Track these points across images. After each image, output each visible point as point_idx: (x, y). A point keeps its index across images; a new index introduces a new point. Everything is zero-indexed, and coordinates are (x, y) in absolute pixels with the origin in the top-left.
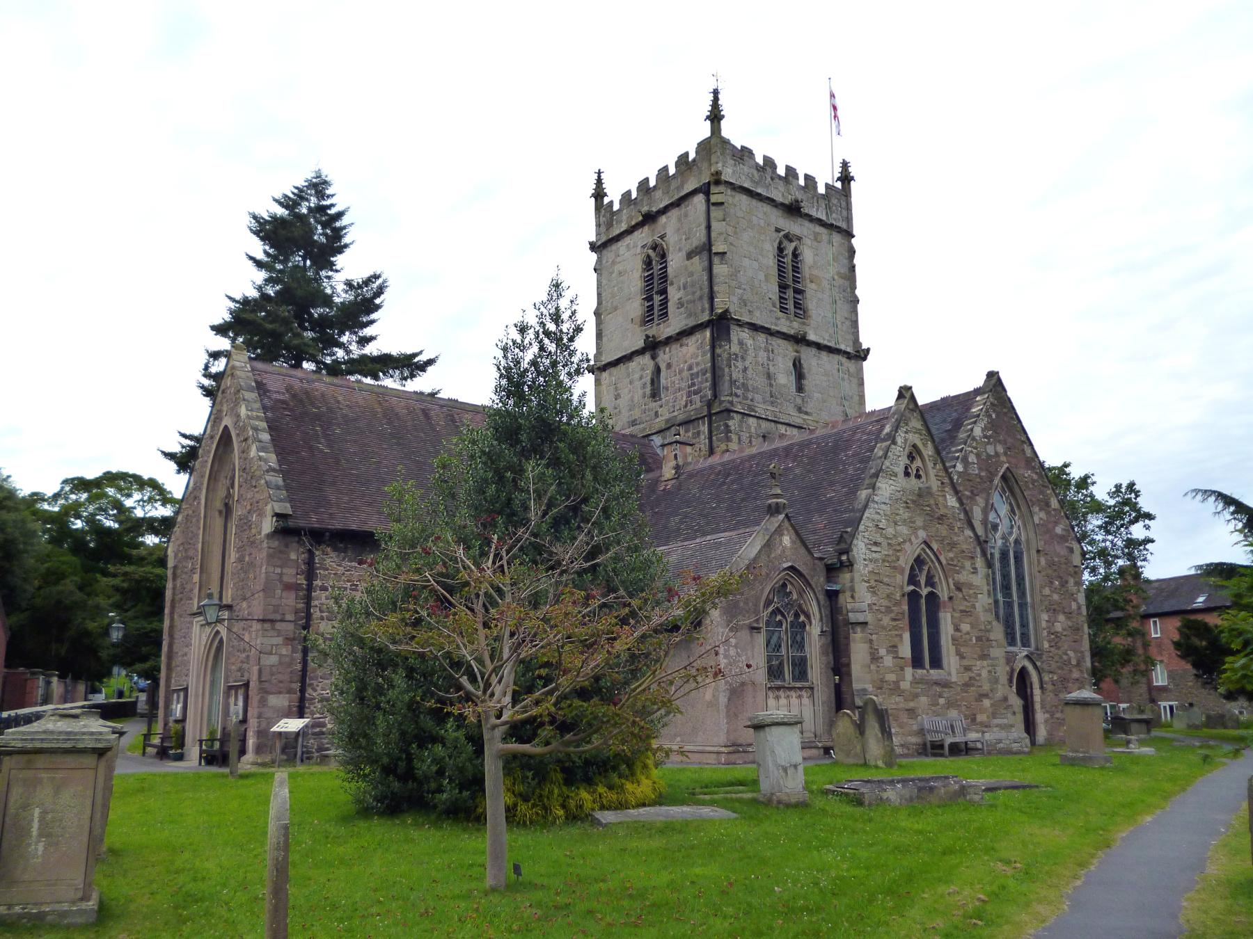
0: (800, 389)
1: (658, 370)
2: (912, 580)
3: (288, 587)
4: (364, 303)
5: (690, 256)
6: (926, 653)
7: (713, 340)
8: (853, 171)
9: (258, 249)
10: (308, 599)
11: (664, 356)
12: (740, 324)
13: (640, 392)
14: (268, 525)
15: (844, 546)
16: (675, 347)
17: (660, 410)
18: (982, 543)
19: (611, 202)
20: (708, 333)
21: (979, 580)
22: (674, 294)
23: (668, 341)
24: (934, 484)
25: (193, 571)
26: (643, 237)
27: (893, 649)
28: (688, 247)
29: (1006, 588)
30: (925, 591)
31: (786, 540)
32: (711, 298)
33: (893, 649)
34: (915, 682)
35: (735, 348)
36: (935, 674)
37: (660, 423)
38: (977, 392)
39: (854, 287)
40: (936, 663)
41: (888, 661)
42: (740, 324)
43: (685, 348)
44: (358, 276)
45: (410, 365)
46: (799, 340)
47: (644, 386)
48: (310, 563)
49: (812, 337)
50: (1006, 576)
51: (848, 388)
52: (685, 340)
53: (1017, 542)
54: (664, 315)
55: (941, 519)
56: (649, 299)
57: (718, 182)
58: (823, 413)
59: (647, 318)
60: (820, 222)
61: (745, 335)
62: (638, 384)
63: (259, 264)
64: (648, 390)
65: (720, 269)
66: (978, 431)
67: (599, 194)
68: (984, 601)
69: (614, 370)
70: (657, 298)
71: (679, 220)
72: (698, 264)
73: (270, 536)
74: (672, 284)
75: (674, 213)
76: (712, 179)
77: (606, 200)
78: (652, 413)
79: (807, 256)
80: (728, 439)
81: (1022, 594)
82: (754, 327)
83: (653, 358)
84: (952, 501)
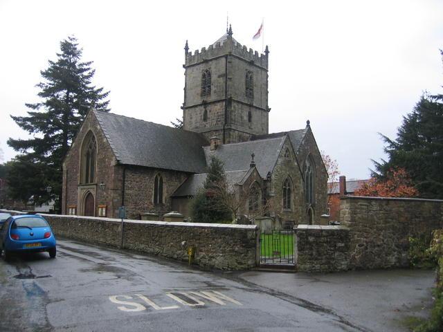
0: (250, 121)
1: (206, 112)
2: (285, 185)
3: (120, 180)
5: (219, 77)
6: (287, 204)
10: (124, 184)
11: (209, 108)
14: (113, 163)
20: (224, 103)
21: (301, 185)
22: (213, 89)
23: (210, 103)
25: (77, 172)
26: (202, 67)
28: (218, 74)
29: (307, 187)
30: (288, 188)
34: (284, 212)
35: (233, 108)
36: (289, 210)
39: (267, 88)
40: (289, 208)
41: (278, 206)
46: (251, 106)
48: (124, 174)
49: (254, 105)
50: (307, 183)
51: (264, 121)
52: (216, 104)
53: (311, 174)
55: (293, 168)
56: (203, 88)
57: (230, 55)
60: (258, 67)
65: (229, 83)
67: (187, 48)
68: (302, 190)
69: (191, 110)
71: (216, 64)
72: (222, 80)
73: (115, 166)
75: (214, 62)
77: (189, 51)
79: (254, 78)
80: (230, 137)
81: (311, 188)
83: (205, 108)
84: (296, 164)
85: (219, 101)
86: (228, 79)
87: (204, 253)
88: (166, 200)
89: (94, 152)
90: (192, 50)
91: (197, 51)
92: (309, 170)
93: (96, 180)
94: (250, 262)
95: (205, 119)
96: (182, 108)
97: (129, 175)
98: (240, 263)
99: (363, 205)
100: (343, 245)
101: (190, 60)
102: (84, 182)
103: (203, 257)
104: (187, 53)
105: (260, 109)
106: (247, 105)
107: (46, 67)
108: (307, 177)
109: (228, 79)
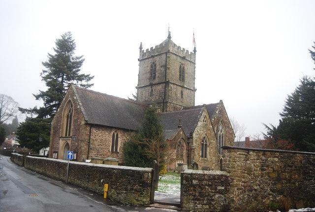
0: (182, 97)
1: (152, 90)
4: (80, 64)
6: (204, 155)
7: (165, 87)
8: (197, 49)
9: (55, 47)
10: (90, 137)
11: (154, 88)
12: (171, 83)
14: (83, 123)
15: (191, 134)
18: (216, 135)
19: (143, 51)
23: (155, 84)
24: (208, 123)
27: (198, 154)
31: (181, 133)
32: (166, 77)
33: (198, 154)
35: (170, 88)
38: (218, 104)
40: (206, 157)
41: (197, 156)
42: (171, 83)
44: (79, 56)
45: (88, 78)
46: (183, 87)
49: (185, 86)
50: (220, 141)
54: (154, 78)
57: (169, 52)
58: (186, 102)
61: (172, 85)
63: (56, 51)
66: (217, 112)
67: (141, 48)
70: (153, 75)
72: (163, 69)
79: (186, 68)
82: (174, 84)
83: (151, 88)
84: (211, 127)
85: (160, 84)
86: (165, 68)
87: (114, 190)
88: (120, 150)
89: (71, 115)
90: (144, 49)
91: (147, 50)
92: (221, 132)
93: (71, 135)
94: (144, 200)
95: (151, 94)
96: (137, 88)
97: (94, 130)
98: (138, 200)
99: (242, 155)
100: (223, 188)
101: (143, 56)
102: (64, 136)
103: (113, 194)
104: (140, 51)
105: (189, 89)
106: (180, 86)
107: (47, 60)
108: (220, 137)
109: (165, 68)
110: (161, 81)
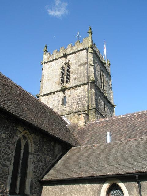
1: (65, 97)
5: (79, 66)
11: (67, 93)
13: (57, 103)
16: (72, 90)
17: (65, 109)
22: (72, 76)
26: (63, 60)
28: (79, 63)
37: (64, 113)
43: (76, 91)
47: (59, 101)
52: (76, 88)
54: (68, 80)
59: (62, 81)
62: (57, 101)
64: (61, 102)
71: (76, 56)
74: (72, 73)
75: (74, 55)
76: (90, 46)
78: (62, 110)
88: (32, 182)
110: (79, 83)
